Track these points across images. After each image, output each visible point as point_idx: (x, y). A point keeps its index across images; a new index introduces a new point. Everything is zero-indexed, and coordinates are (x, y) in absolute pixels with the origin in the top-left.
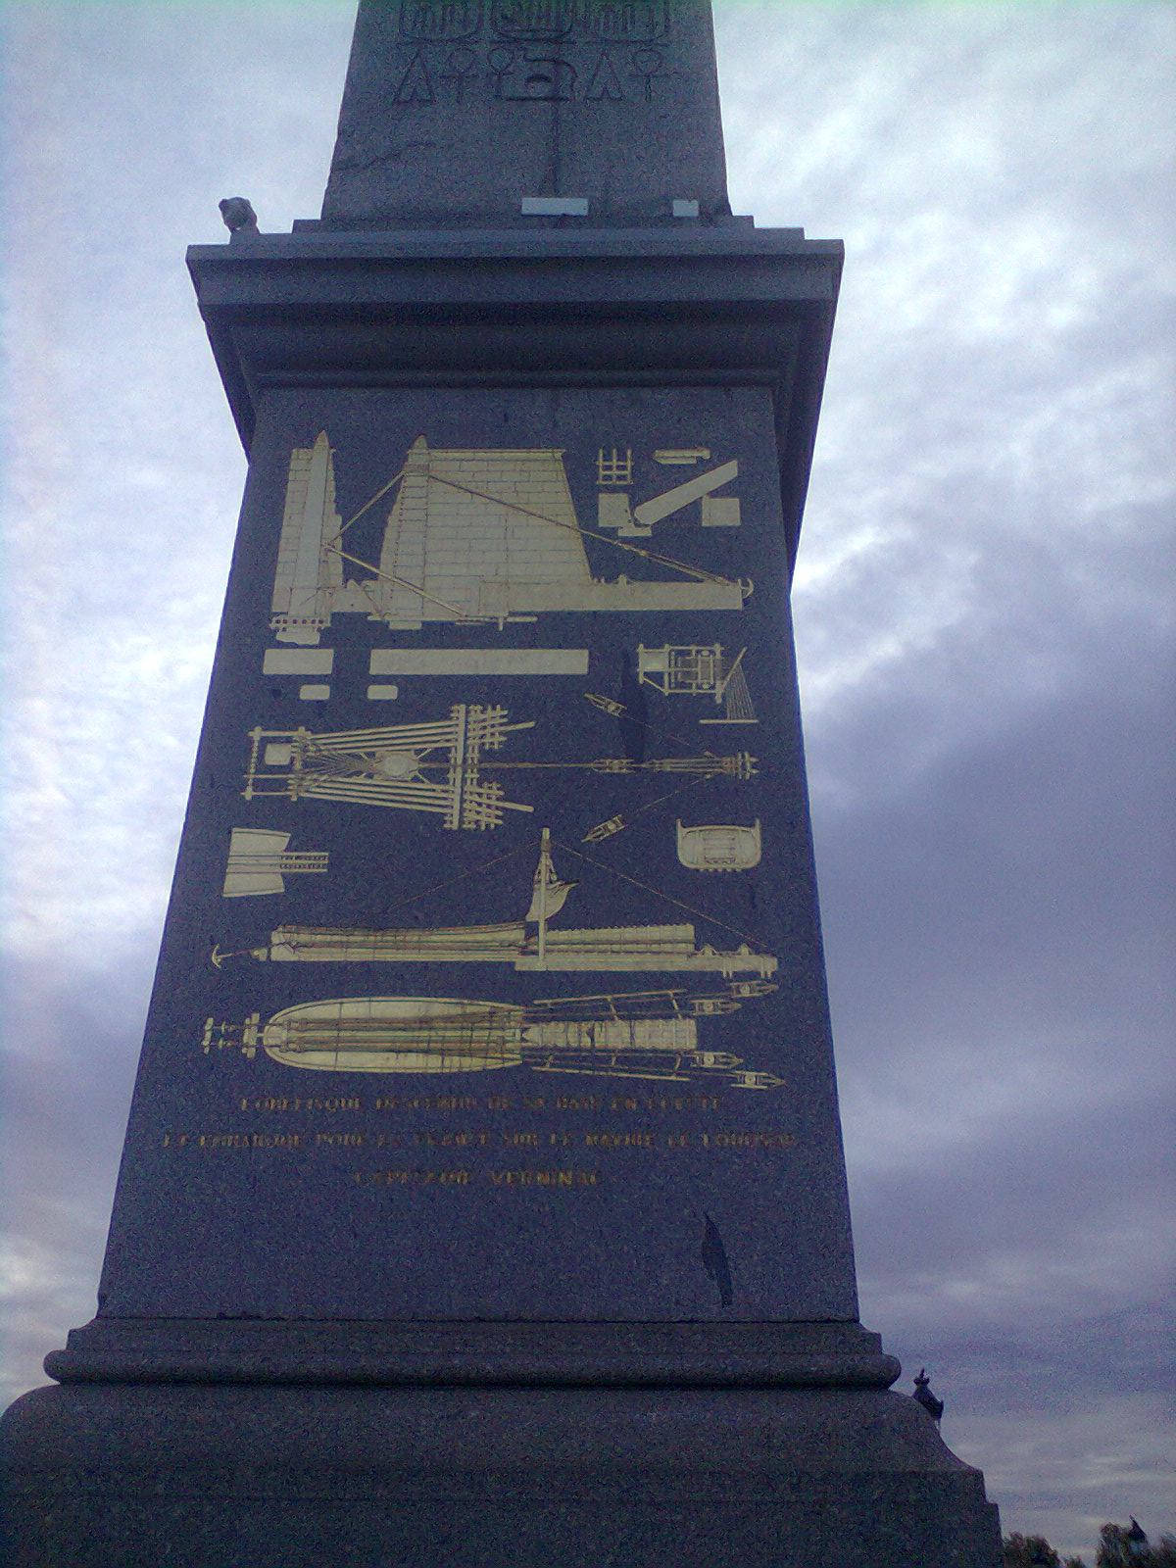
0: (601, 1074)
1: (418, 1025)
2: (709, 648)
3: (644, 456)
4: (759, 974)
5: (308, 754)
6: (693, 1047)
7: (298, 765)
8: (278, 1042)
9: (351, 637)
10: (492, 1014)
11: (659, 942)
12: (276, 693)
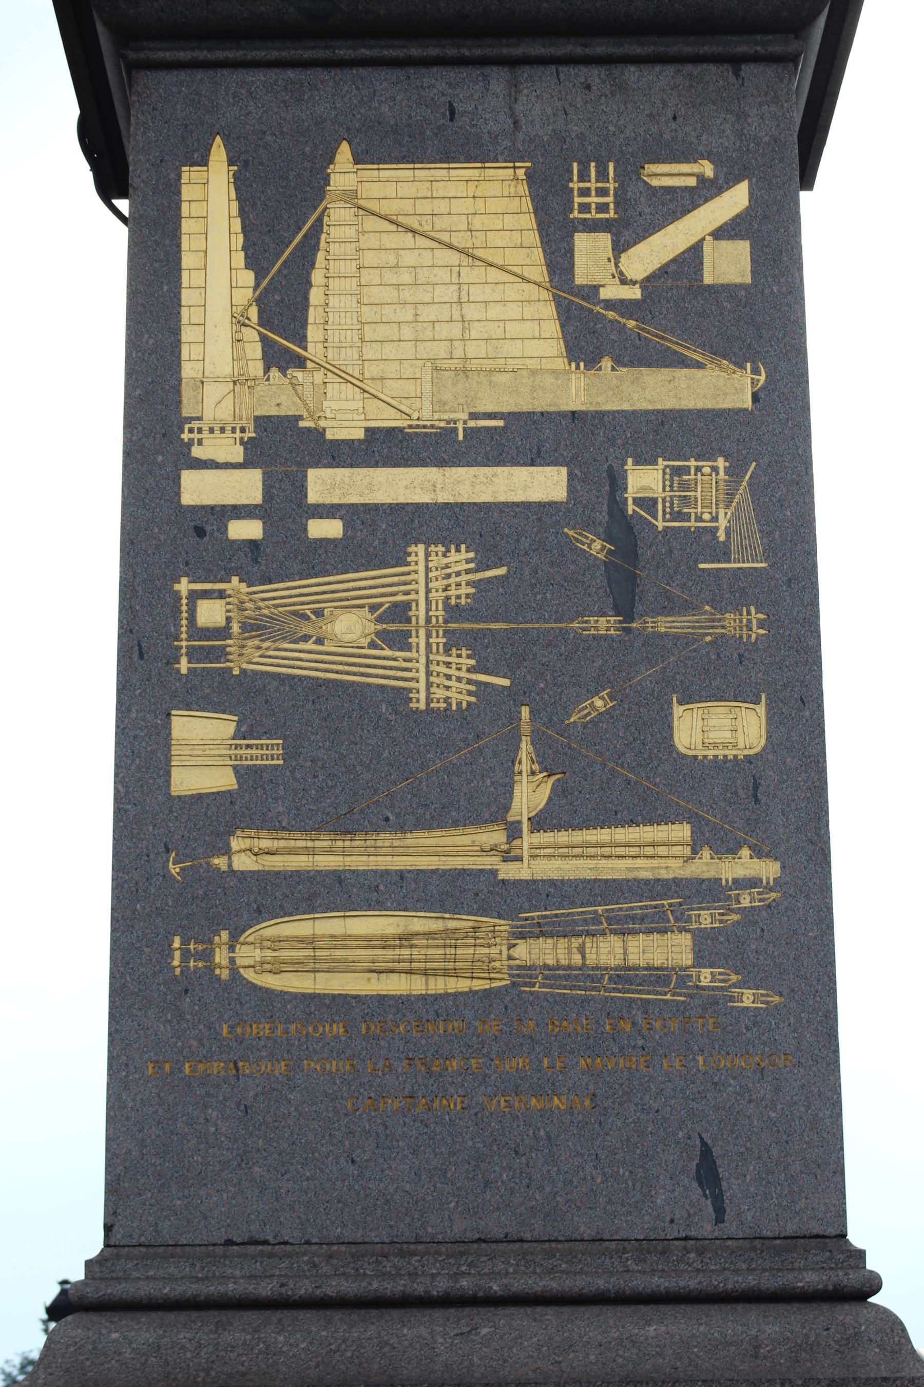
0: (593, 993)
1: (397, 942)
2: (710, 463)
4: (761, 880)
5: (246, 613)
6: (690, 963)
7: (235, 628)
8: (252, 963)
9: (284, 448)
10: (475, 929)
11: (653, 845)
12: (200, 532)
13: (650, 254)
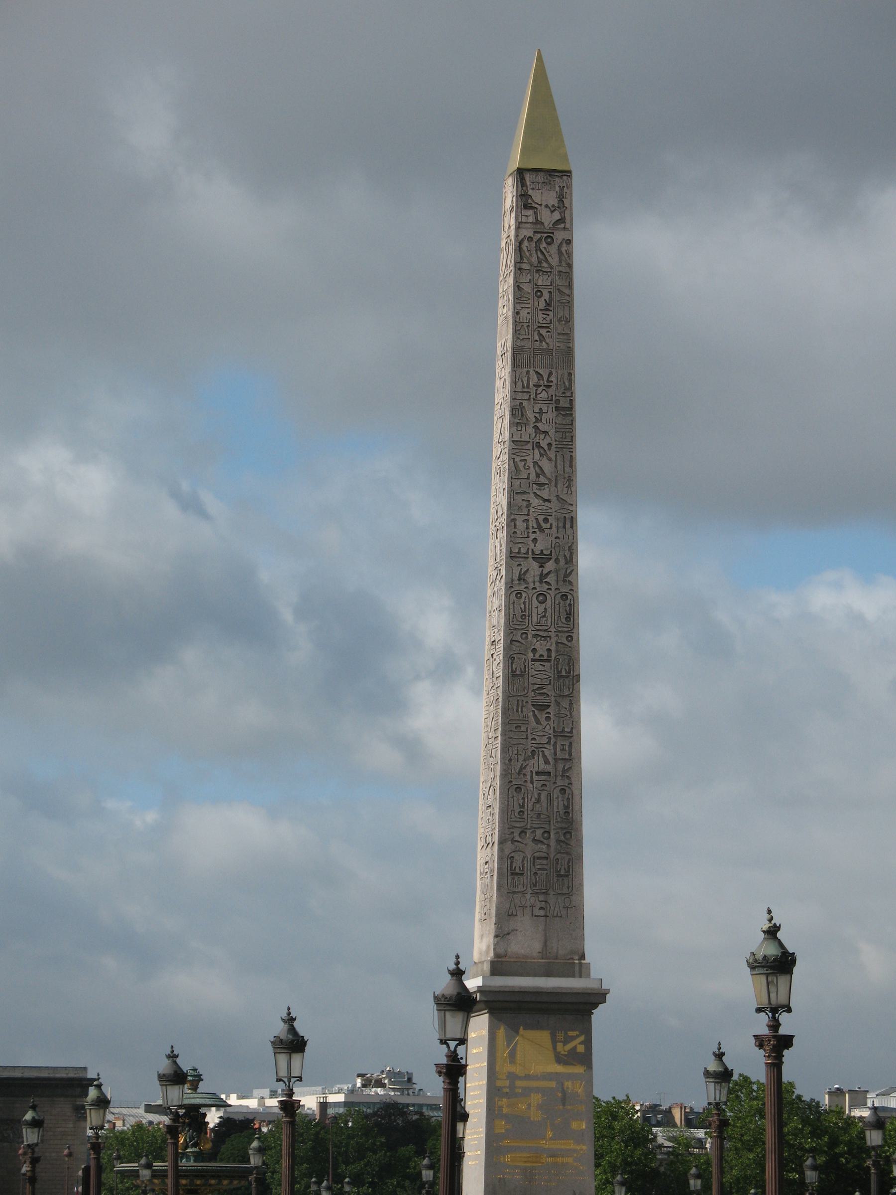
3: (566, 1034)
13: (569, 1046)
